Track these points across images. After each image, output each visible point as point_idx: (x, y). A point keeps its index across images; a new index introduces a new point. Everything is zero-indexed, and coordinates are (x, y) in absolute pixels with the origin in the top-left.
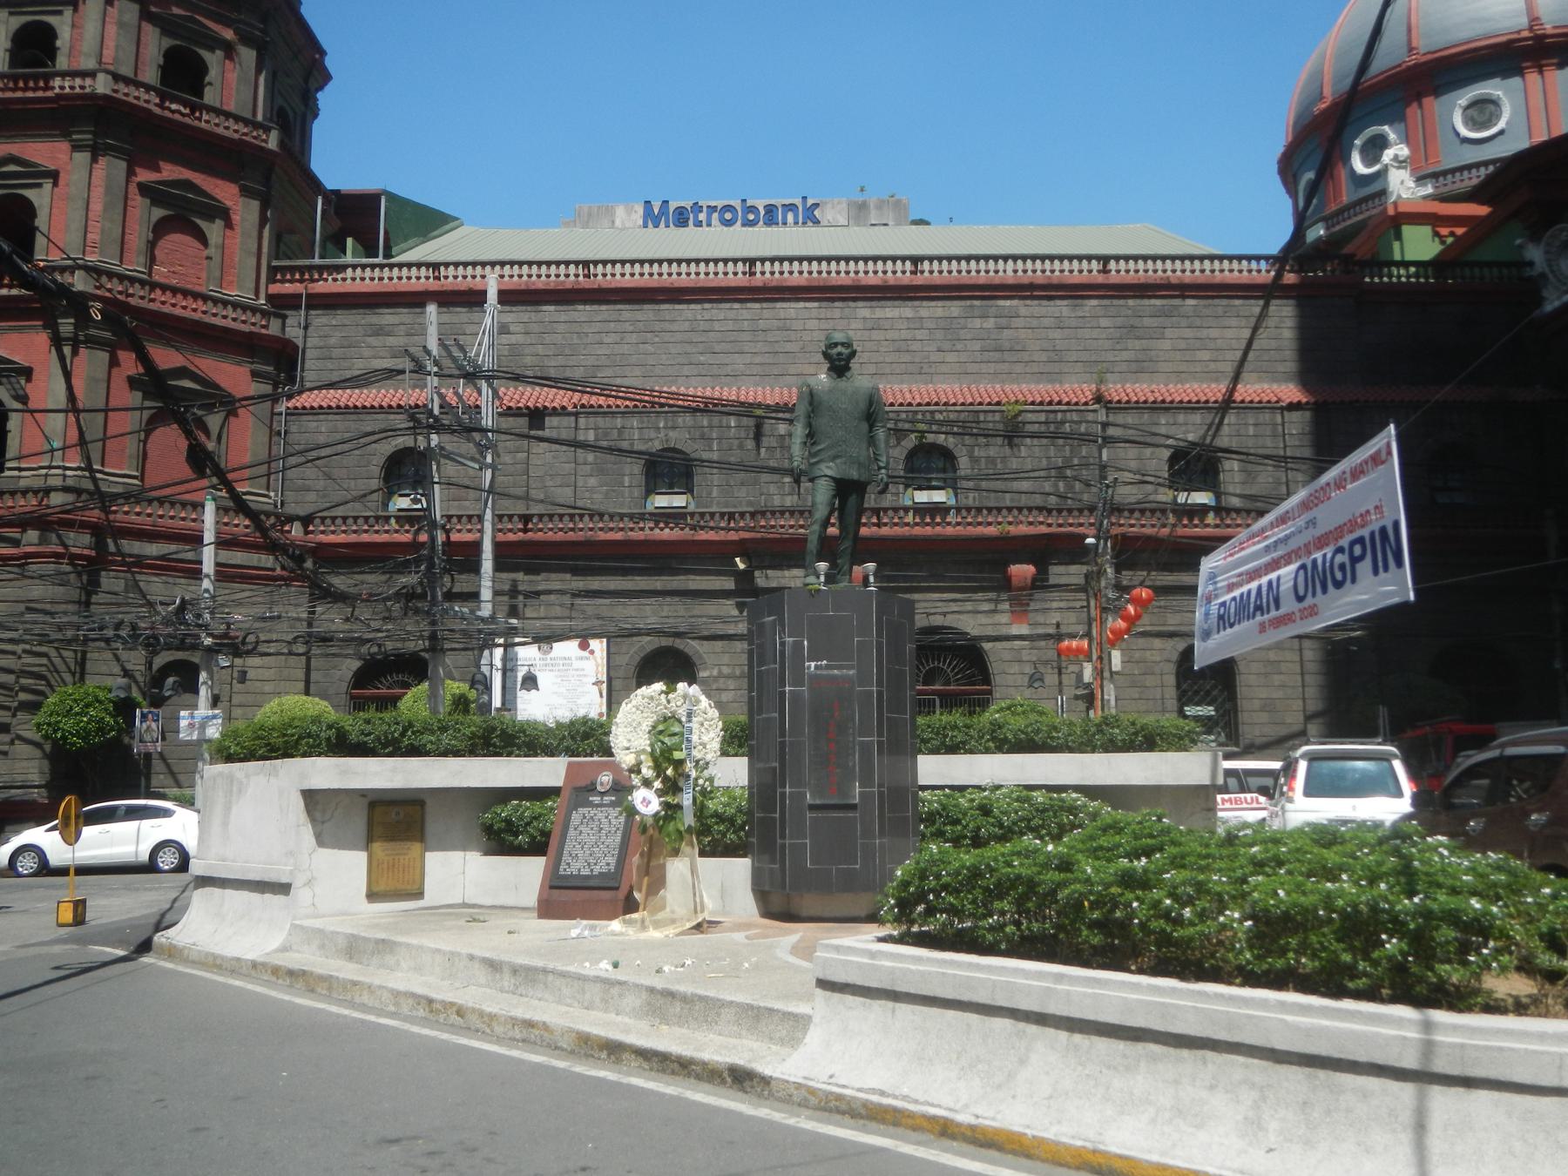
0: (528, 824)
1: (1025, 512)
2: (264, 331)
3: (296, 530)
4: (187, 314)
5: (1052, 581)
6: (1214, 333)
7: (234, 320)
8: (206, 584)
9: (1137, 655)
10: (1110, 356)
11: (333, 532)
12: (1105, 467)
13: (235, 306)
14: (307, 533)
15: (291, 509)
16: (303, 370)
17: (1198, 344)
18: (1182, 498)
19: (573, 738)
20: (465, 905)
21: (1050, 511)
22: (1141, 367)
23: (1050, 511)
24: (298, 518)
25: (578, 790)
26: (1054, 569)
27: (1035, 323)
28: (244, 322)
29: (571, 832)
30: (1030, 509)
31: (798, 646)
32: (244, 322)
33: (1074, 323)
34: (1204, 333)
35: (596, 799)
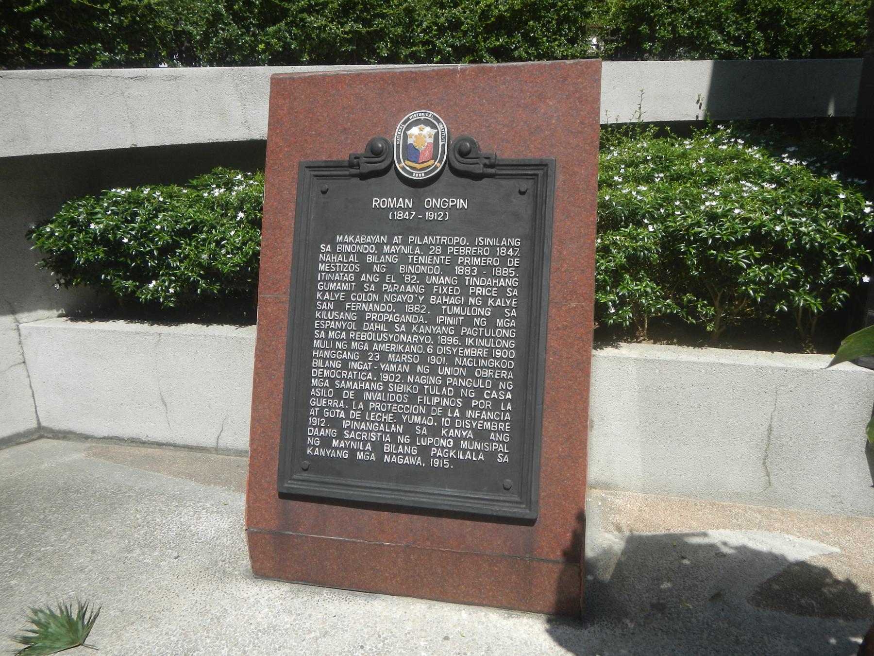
0: (168, 250)
20: (41, 432)
25: (324, 172)
29: (328, 321)
35: (399, 205)
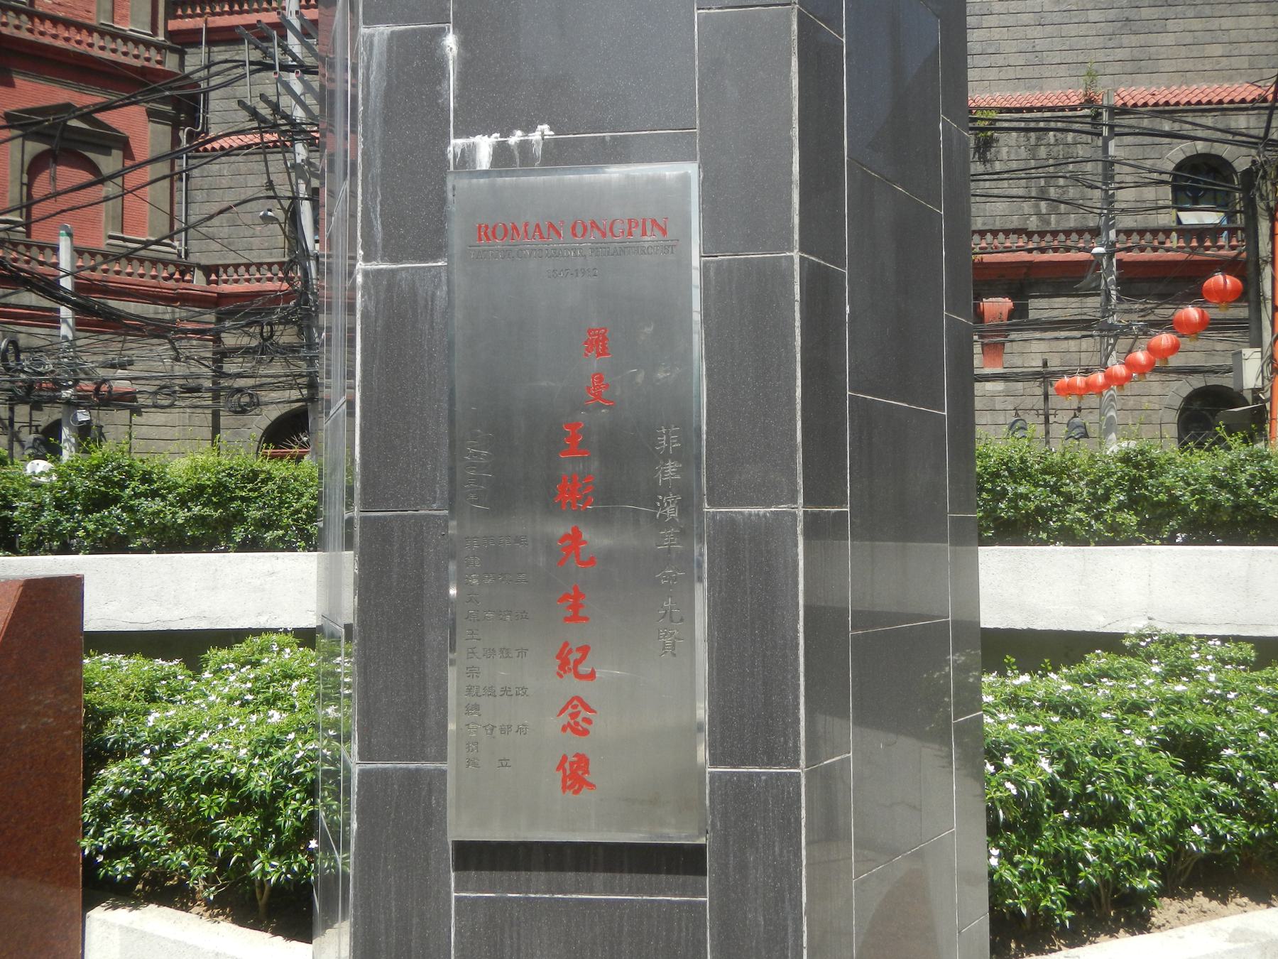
1: (1001, 236)
2: (158, 67)
3: (198, 281)
4: (71, 46)
5: (1033, 315)
6: (1227, 23)
7: (125, 54)
8: (65, 330)
9: (1131, 403)
10: (1101, 55)
11: (236, 281)
12: (1112, 163)
13: (126, 39)
14: (209, 282)
15: (193, 259)
16: (206, 111)
17: (1208, 37)
18: (1189, 218)
19: (60, 505)
21: (1030, 235)
22: (1137, 67)
23: (1030, 235)
24: (200, 267)
26: (1033, 303)
27: (1011, 20)
28: (137, 57)
30: (1007, 232)
31: (415, 62)
32: (137, 57)
33: (1057, 18)
34: (1215, 24)
